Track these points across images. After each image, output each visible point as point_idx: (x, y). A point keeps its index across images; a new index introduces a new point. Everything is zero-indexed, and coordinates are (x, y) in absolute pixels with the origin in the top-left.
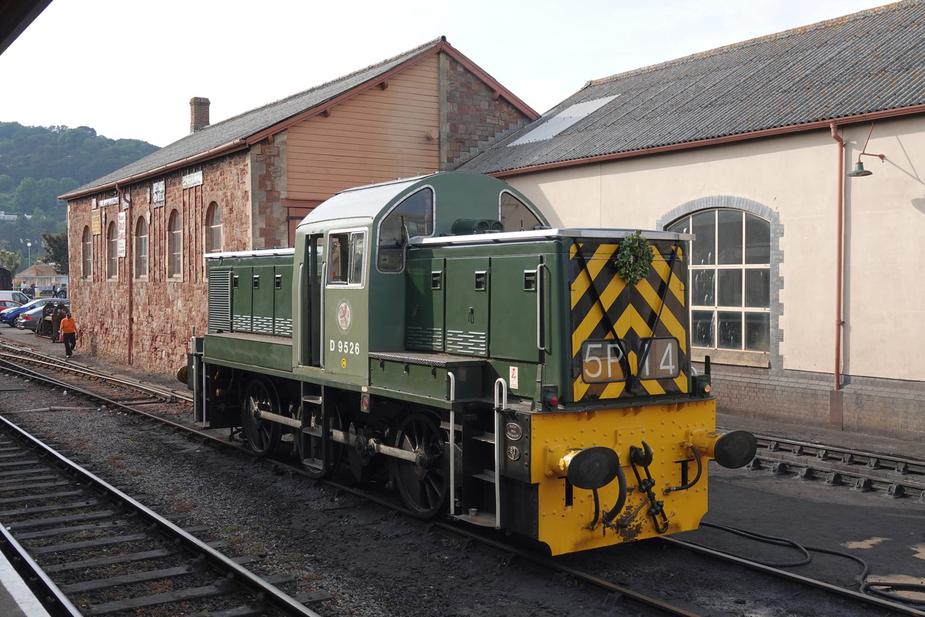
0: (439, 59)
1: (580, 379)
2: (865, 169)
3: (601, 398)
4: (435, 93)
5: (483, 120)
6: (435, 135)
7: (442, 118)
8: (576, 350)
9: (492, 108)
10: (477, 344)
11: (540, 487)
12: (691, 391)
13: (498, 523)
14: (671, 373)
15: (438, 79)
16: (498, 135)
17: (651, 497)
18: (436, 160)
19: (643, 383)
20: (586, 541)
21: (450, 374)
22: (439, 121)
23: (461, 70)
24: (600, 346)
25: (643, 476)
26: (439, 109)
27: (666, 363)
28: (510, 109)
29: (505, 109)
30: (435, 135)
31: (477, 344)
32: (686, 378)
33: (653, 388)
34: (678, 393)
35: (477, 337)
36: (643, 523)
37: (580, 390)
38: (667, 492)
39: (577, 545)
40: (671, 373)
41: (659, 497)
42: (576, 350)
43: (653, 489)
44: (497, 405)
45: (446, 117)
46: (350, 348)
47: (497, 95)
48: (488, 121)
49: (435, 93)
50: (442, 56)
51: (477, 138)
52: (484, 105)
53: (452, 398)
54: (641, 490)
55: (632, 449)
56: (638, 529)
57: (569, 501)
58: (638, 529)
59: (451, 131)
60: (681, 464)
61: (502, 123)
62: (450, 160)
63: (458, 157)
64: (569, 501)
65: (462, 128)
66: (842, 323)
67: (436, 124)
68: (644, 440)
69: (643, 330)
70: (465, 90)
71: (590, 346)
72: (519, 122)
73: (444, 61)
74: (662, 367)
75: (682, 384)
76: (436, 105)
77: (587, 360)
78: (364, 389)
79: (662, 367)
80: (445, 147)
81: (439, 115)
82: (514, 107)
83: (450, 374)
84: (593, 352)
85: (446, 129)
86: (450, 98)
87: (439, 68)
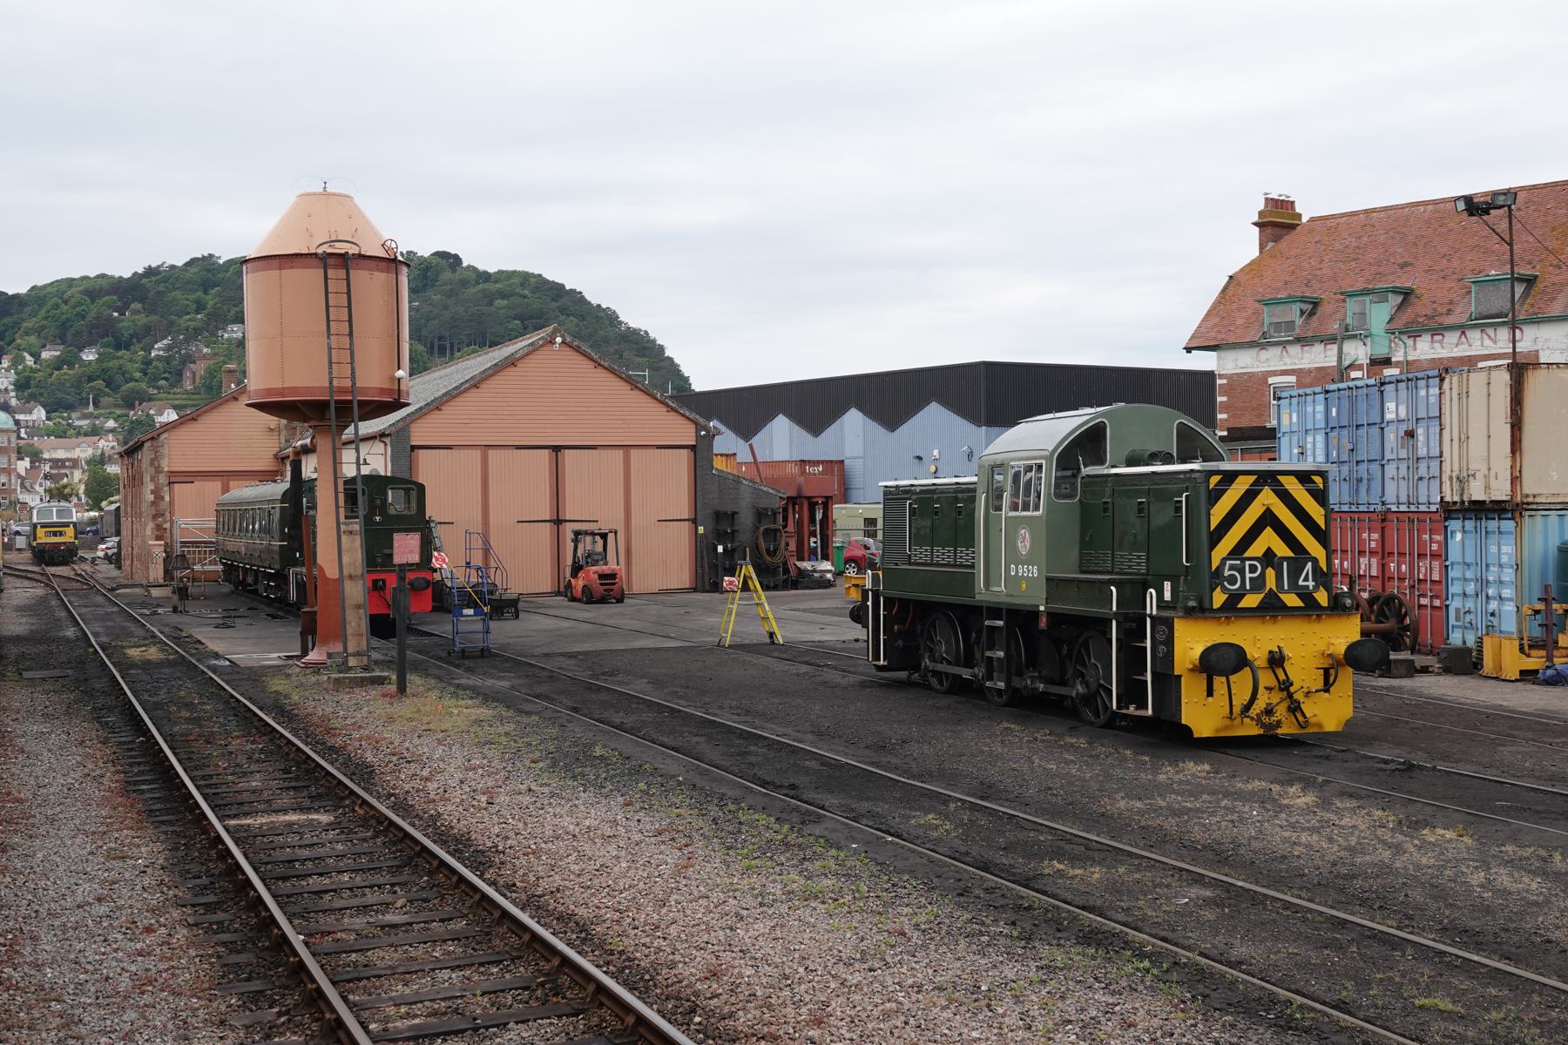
1: (1219, 589)
3: (1239, 606)
8: (1215, 565)
10: (1139, 564)
11: (1183, 679)
12: (1332, 605)
13: (1150, 712)
14: (1311, 588)
17: (1290, 696)
19: (1282, 596)
20: (1226, 728)
21: (1113, 588)
24: (1238, 562)
25: (1282, 677)
27: (1306, 579)
31: (1139, 564)
32: (1326, 594)
33: (1292, 600)
34: (1317, 605)
35: (1139, 557)
36: (1283, 719)
37: (1219, 599)
38: (1308, 694)
39: (1217, 731)
40: (1311, 588)
41: (1299, 696)
42: (1215, 565)
43: (1292, 689)
44: (1148, 612)
46: (1029, 571)
53: (1114, 609)
54: (1282, 690)
55: (1270, 652)
56: (1279, 724)
57: (1210, 693)
58: (1279, 724)
60: (1322, 671)
64: (1210, 693)
68: (1282, 645)
69: (1282, 550)
71: (1228, 562)
74: (1301, 583)
75: (1322, 597)
77: (1227, 573)
78: (1042, 608)
79: (1301, 583)
83: (1113, 588)
84: (1232, 568)
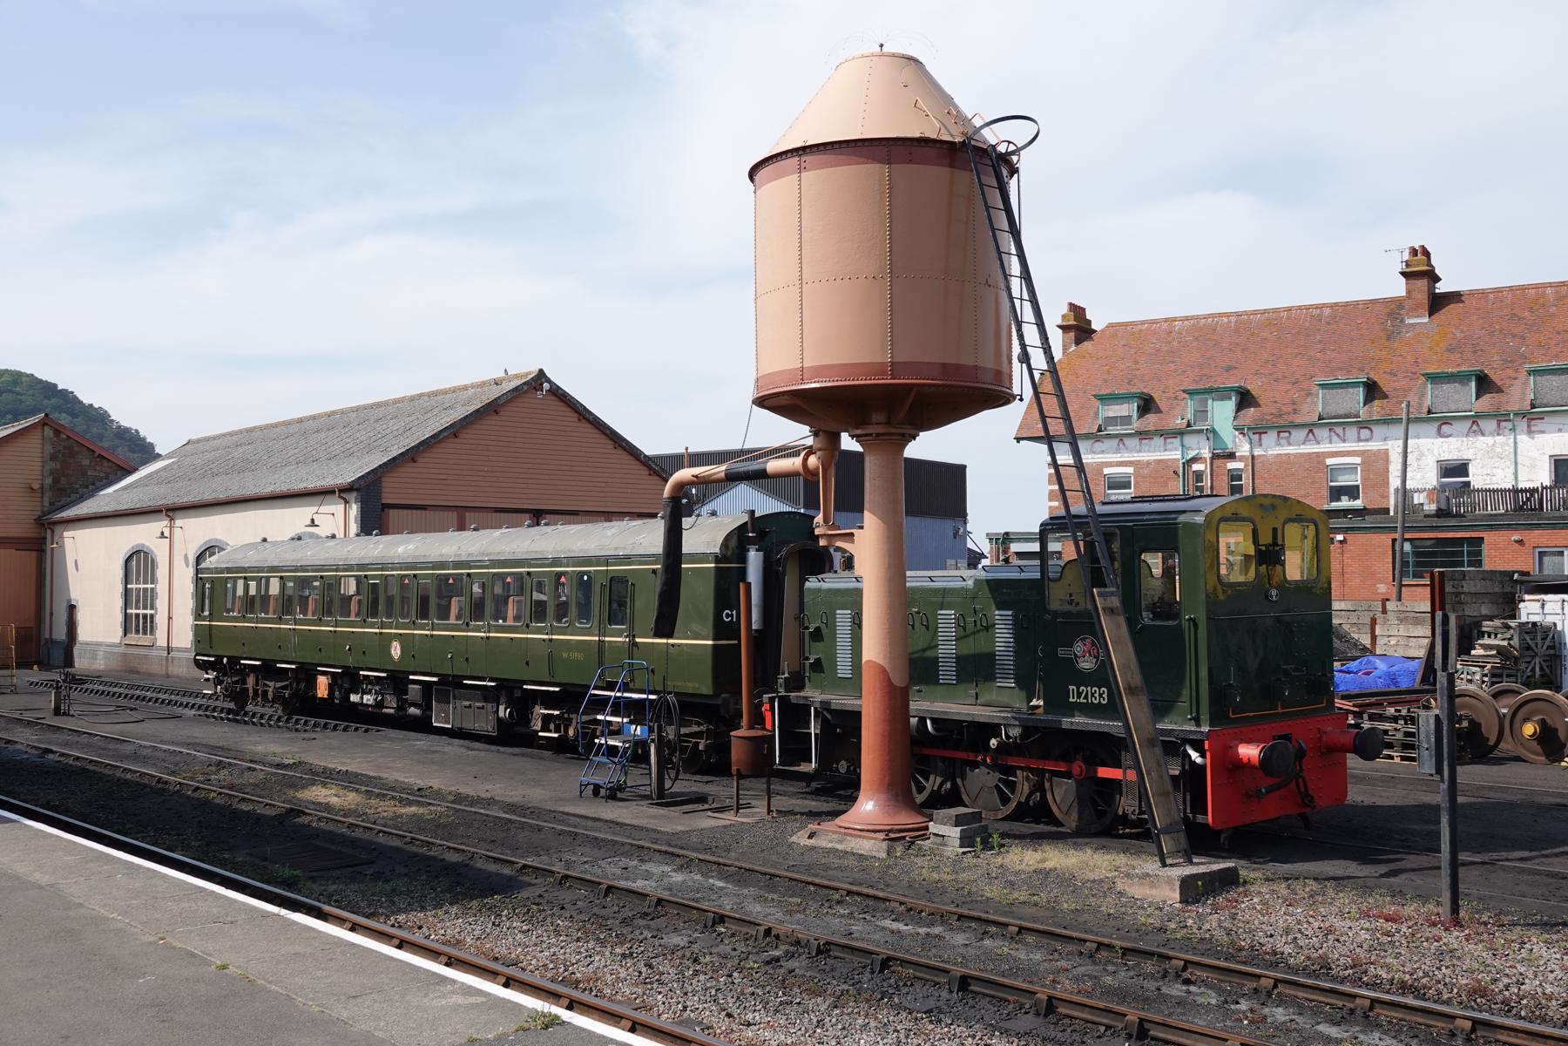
0: (43, 429)
2: (316, 523)
4: (40, 455)
5: (84, 474)
6: (36, 486)
7: (45, 474)
9: (93, 464)
15: (43, 444)
16: (98, 484)
18: (38, 504)
22: (43, 475)
23: (64, 436)
26: (43, 466)
28: (110, 464)
29: (106, 464)
30: (36, 486)
45: (48, 472)
47: (96, 455)
48: (89, 473)
49: (40, 455)
50: (46, 428)
51: (78, 486)
52: (86, 462)
59: (53, 482)
61: (102, 475)
62: (51, 504)
63: (60, 501)
65: (63, 481)
66: (170, 618)
67: (40, 477)
70: (67, 451)
72: (119, 473)
73: (48, 432)
76: (40, 464)
80: (48, 495)
81: (42, 471)
82: (114, 463)
85: (49, 481)
86: (53, 458)
87: (43, 436)
